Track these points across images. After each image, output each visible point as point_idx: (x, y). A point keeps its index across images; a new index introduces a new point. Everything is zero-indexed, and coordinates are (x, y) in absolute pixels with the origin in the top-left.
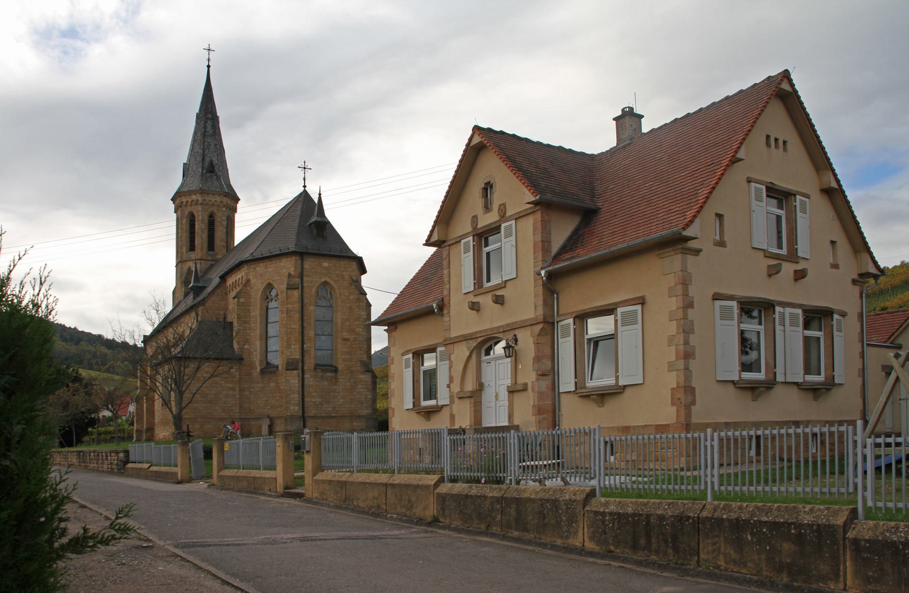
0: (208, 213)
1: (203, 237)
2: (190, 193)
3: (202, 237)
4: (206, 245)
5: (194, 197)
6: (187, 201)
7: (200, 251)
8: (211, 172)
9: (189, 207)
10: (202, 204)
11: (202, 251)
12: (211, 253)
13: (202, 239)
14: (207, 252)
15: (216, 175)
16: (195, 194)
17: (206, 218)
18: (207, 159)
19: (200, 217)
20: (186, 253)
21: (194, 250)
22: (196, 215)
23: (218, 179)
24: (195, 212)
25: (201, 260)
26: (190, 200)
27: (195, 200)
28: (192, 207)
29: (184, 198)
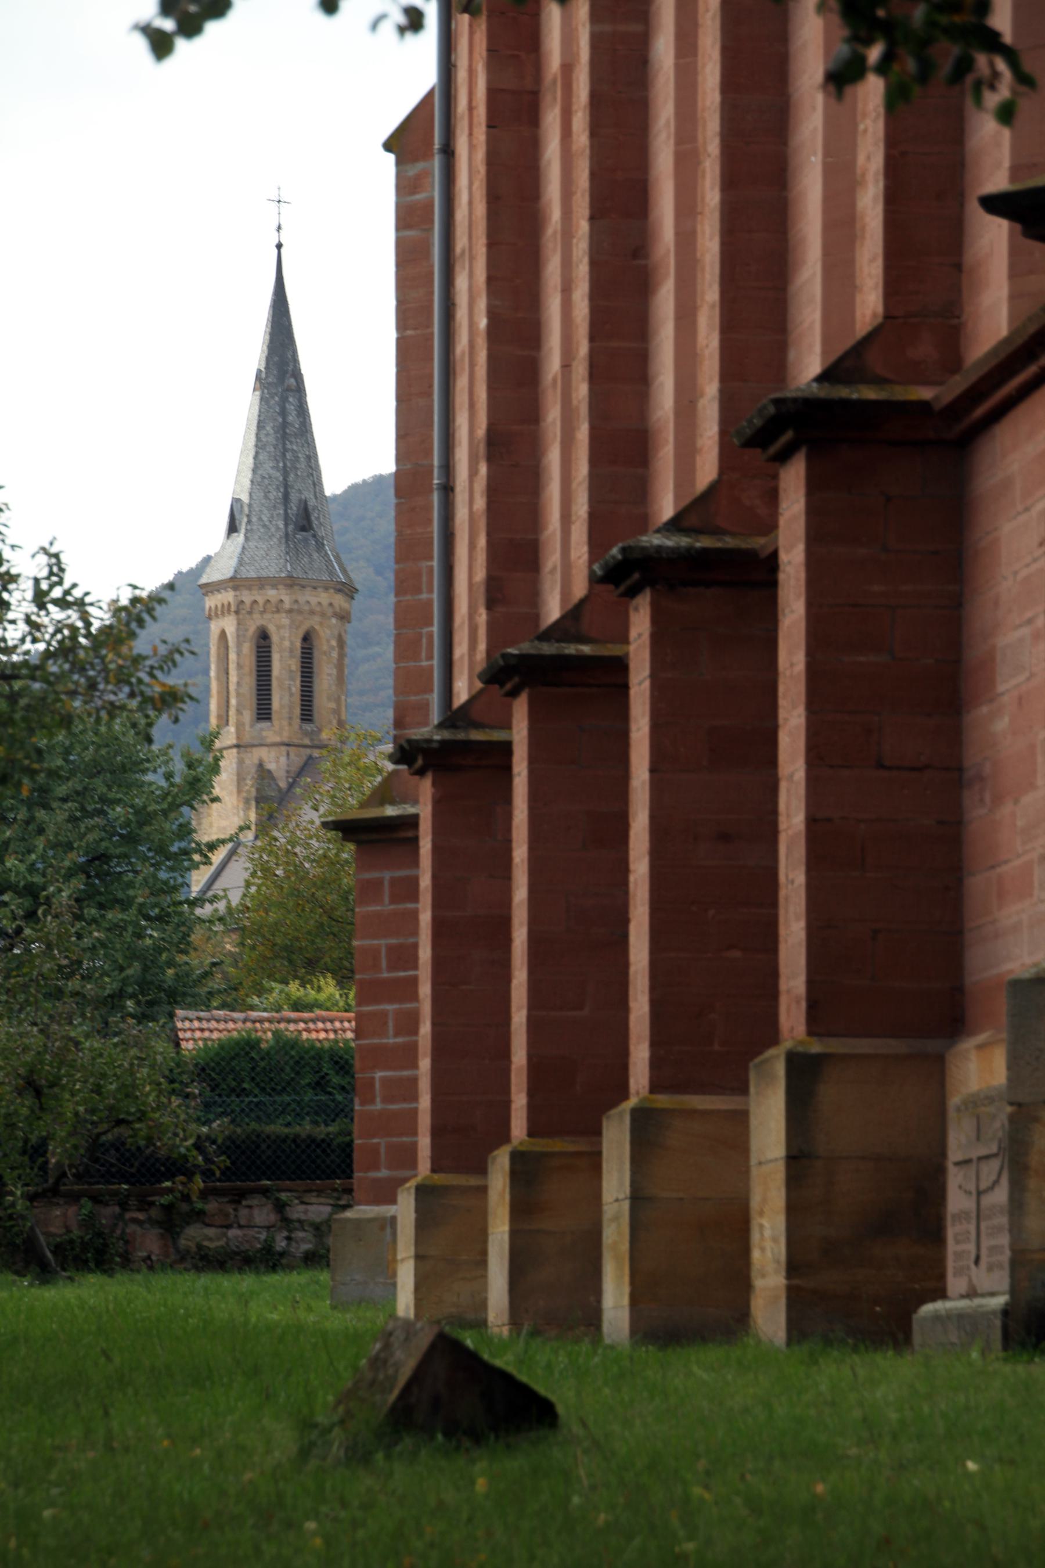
0: (301, 633)
1: (294, 689)
2: (261, 583)
3: (290, 689)
4: (297, 711)
5: (272, 594)
6: (255, 602)
7: (285, 723)
8: (303, 529)
9: (256, 616)
10: (290, 611)
11: (290, 724)
12: (308, 727)
13: (291, 695)
14: (301, 728)
15: (314, 536)
16: (274, 586)
17: (298, 644)
18: (294, 497)
19: (287, 644)
20: (252, 726)
21: (269, 719)
22: (275, 638)
23: (320, 546)
24: (272, 629)
25: (288, 745)
26: (261, 600)
27: (273, 600)
28: (268, 616)
29: (246, 592)
